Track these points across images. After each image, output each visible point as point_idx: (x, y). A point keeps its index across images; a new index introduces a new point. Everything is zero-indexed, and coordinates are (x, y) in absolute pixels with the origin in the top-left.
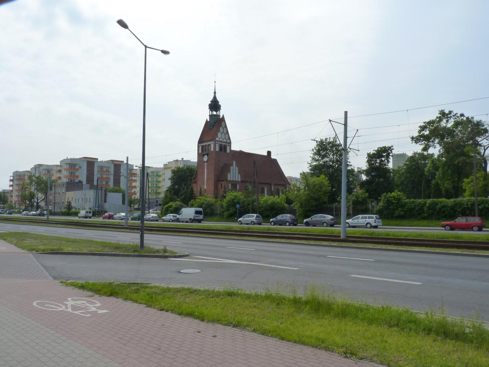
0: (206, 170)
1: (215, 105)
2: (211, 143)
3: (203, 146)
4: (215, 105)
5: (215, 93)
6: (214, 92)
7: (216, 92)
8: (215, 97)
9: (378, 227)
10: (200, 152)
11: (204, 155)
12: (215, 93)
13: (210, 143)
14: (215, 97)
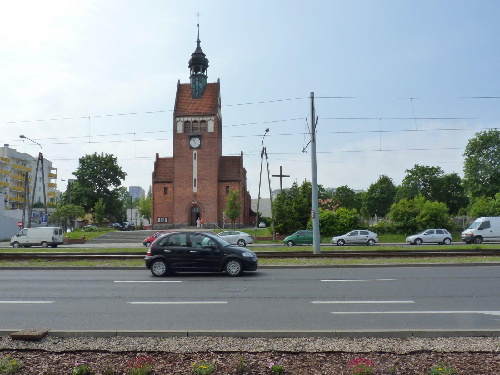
1: (198, 62)
2: (209, 118)
3: (186, 123)
4: (198, 62)
5: (199, 42)
6: (197, 40)
7: (200, 40)
9: (437, 243)
10: (180, 129)
11: (191, 137)
12: (199, 42)
13: (205, 119)
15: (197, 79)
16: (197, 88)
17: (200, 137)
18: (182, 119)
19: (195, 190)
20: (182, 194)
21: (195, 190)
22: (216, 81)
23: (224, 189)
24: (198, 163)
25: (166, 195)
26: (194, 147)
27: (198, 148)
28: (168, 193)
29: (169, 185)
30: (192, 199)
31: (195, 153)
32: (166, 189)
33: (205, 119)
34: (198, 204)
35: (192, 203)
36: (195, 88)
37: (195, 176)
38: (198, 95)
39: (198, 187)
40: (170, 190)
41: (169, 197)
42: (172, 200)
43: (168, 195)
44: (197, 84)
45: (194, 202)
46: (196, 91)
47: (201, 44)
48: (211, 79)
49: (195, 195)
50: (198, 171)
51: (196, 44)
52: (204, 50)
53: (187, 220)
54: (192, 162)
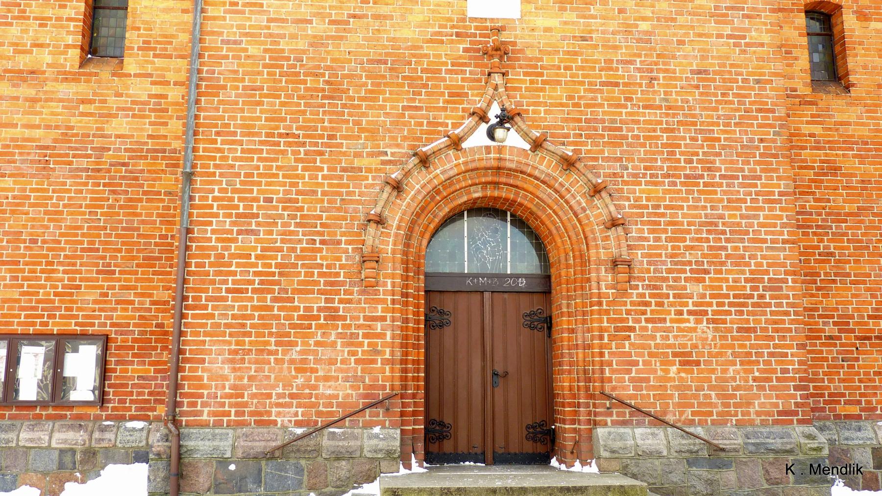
20: (318, 27)
25: (104, 71)
28: (132, 38)
30: (457, 95)
34: (544, 165)
35: (456, 143)
41: (140, 90)
42: (175, 126)
43: (131, 65)
45: (478, 139)
53: (385, 376)
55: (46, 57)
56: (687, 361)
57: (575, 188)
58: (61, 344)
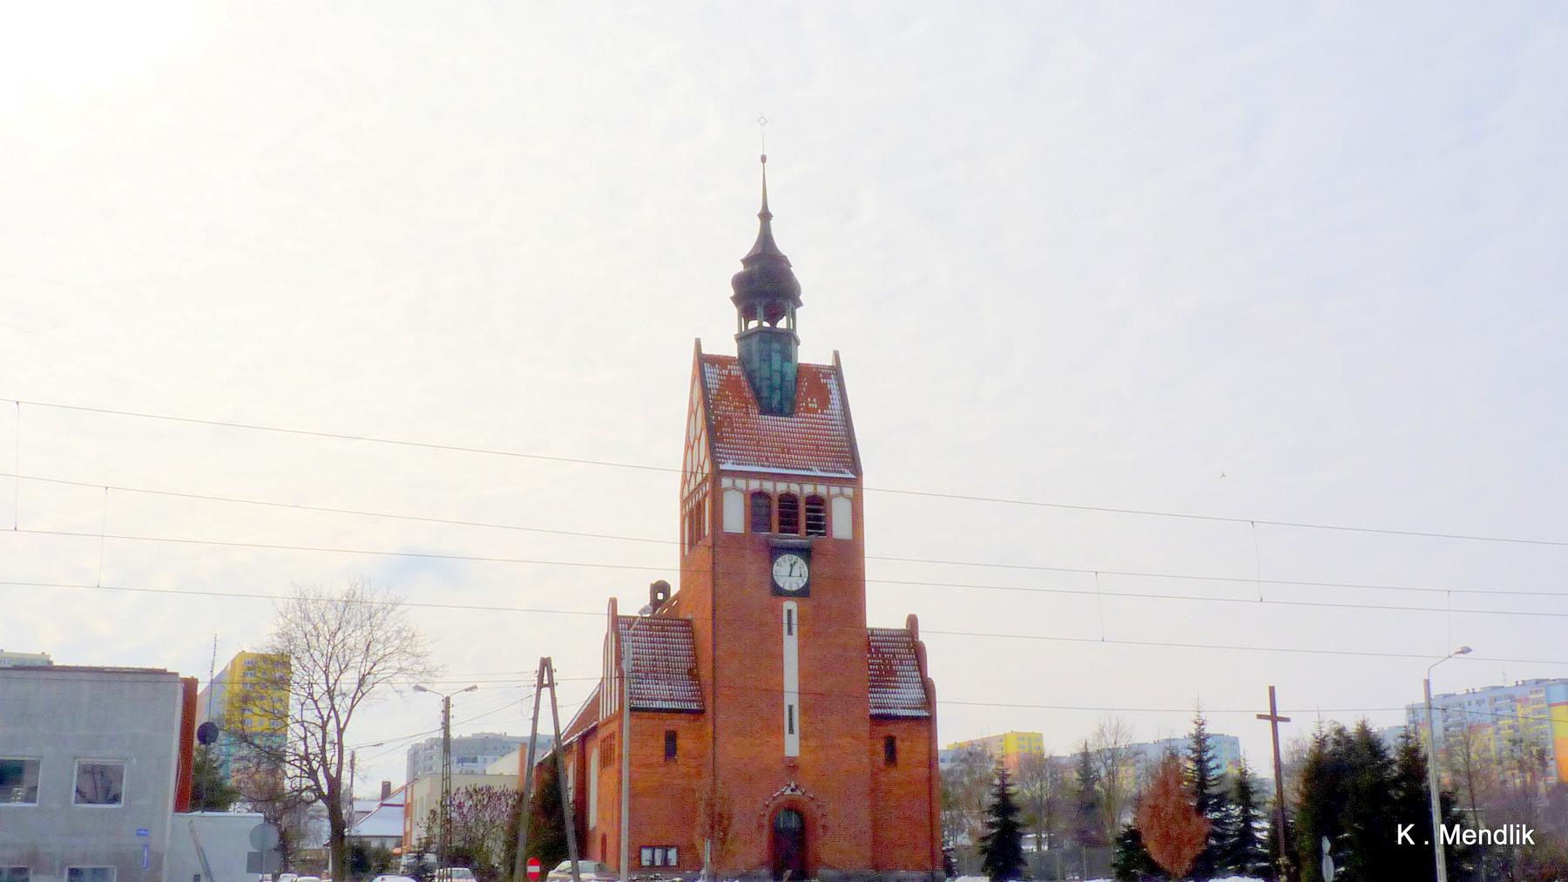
0: (791, 646)
1: (766, 287)
2: (834, 490)
4: (766, 287)
5: (765, 216)
6: (759, 209)
7: (771, 210)
8: (766, 239)
11: (775, 551)
12: (765, 216)
14: (766, 239)
15: (776, 346)
16: (777, 380)
17: (806, 553)
18: (741, 483)
19: (792, 746)
21: (792, 746)
22: (828, 361)
23: (880, 746)
24: (801, 648)
26: (787, 588)
27: (803, 593)
29: (682, 723)
31: (789, 612)
32: (671, 738)
33: (822, 490)
36: (770, 379)
37: (791, 698)
38: (781, 403)
39: (804, 737)
40: (684, 743)
41: (683, 769)
44: (776, 364)
46: (772, 389)
47: (772, 222)
48: (811, 352)
49: (792, 767)
50: (803, 676)
51: (758, 222)
52: (783, 244)
53: (765, 858)
54: (780, 642)
55: (655, 759)
56: (841, 852)
57: (813, 805)
58: (666, 848)
